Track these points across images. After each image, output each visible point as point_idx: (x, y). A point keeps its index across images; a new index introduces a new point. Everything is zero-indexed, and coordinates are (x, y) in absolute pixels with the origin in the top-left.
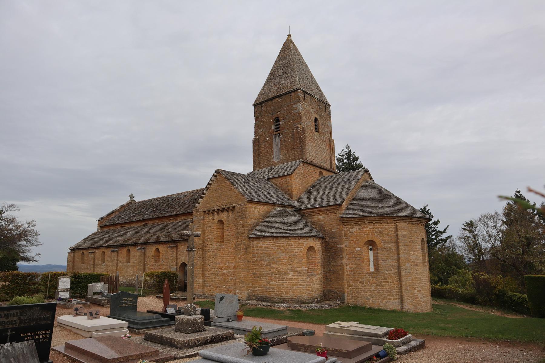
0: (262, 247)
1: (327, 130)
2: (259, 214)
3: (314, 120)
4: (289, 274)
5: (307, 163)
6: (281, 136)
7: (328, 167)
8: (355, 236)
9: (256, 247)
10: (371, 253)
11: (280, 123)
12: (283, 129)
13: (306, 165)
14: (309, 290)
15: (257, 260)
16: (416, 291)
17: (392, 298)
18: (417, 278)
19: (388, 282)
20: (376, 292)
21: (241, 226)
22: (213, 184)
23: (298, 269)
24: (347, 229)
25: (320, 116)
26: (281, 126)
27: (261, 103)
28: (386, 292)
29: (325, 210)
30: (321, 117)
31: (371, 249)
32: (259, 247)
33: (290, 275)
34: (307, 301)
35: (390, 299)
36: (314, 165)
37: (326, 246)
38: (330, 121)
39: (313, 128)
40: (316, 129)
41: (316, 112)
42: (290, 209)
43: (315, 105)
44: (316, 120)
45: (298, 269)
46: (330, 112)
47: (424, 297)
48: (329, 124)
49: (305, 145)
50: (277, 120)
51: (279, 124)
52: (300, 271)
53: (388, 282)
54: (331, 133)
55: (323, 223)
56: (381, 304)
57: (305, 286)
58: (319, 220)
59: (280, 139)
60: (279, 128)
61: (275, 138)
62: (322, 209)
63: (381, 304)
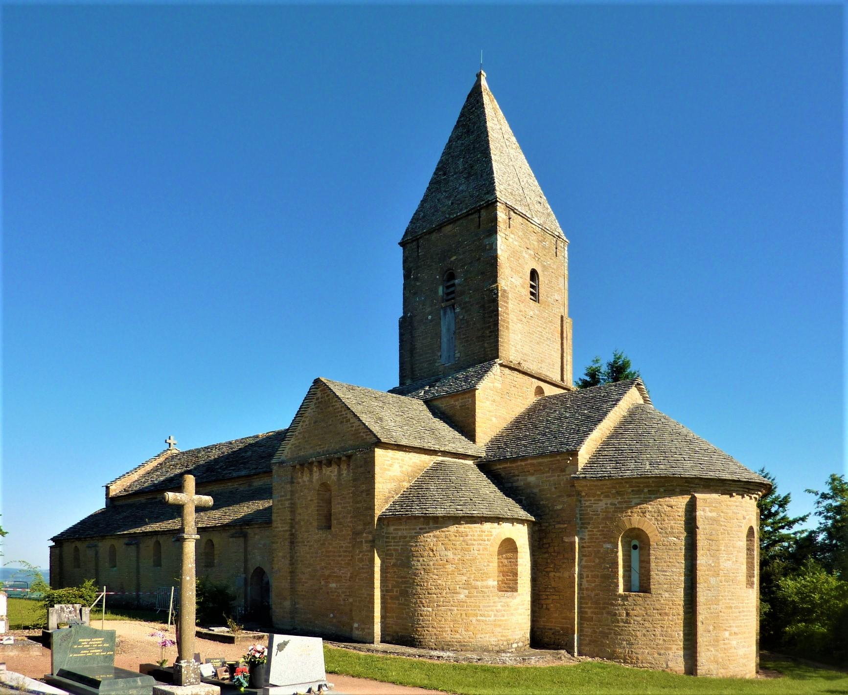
0: (405, 537)
2: (402, 472)
4: (459, 593)
6: (458, 310)
7: (557, 378)
8: (603, 519)
9: (394, 538)
10: (635, 554)
11: (456, 281)
12: (462, 293)
13: (507, 371)
14: (500, 626)
15: (394, 565)
16: (727, 634)
18: (731, 607)
19: (666, 614)
21: (364, 495)
22: (309, 410)
23: (479, 584)
24: (588, 503)
25: (544, 266)
26: (458, 288)
27: (416, 239)
29: (540, 464)
30: (545, 268)
31: (635, 547)
32: (401, 537)
33: (462, 596)
34: (497, 648)
37: (540, 539)
39: (526, 291)
40: (535, 295)
41: (536, 257)
42: (470, 462)
44: (534, 274)
45: (479, 584)
47: (744, 647)
49: (507, 328)
50: (452, 276)
51: (454, 285)
52: (482, 587)
53: (666, 614)
57: (492, 618)
59: (456, 316)
60: (453, 292)
61: (445, 313)
62: (535, 461)
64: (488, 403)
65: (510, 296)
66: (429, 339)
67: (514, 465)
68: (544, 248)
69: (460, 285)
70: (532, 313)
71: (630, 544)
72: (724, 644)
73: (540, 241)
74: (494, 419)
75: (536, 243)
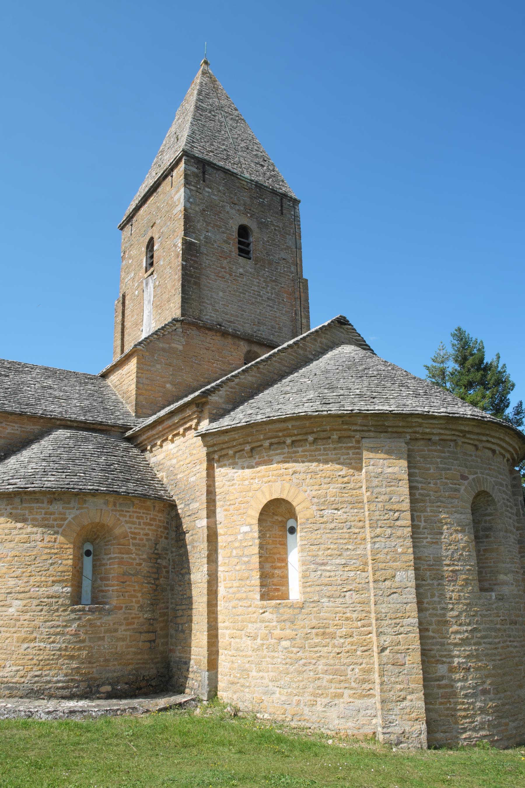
1: (283, 255)
3: (235, 229)
5: (198, 327)
11: (155, 248)
12: (159, 258)
13: (193, 332)
17: (347, 692)
20: (292, 669)
28: (326, 672)
30: (262, 225)
33: (11, 610)
35: (341, 696)
36: (225, 334)
38: (297, 236)
39: (233, 248)
40: (244, 251)
43: (245, 197)
44: (244, 232)
46: (296, 218)
48: (290, 243)
50: (151, 243)
54: (298, 264)
55: (174, 461)
56: (306, 710)
58: (169, 457)
63: (306, 710)
64: (159, 366)
65: (204, 250)
66: (135, 316)
67: (154, 432)
68: (262, 204)
69: (157, 250)
70: (241, 270)
71: (284, 527)
72: (439, 687)
73: (251, 198)
74: (168, 386)
75: (248, 200)
